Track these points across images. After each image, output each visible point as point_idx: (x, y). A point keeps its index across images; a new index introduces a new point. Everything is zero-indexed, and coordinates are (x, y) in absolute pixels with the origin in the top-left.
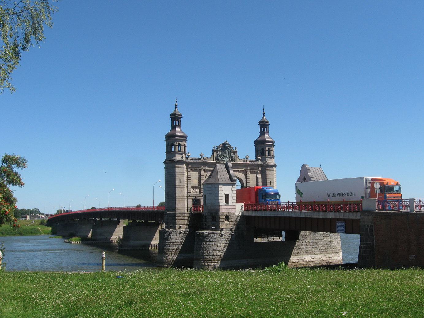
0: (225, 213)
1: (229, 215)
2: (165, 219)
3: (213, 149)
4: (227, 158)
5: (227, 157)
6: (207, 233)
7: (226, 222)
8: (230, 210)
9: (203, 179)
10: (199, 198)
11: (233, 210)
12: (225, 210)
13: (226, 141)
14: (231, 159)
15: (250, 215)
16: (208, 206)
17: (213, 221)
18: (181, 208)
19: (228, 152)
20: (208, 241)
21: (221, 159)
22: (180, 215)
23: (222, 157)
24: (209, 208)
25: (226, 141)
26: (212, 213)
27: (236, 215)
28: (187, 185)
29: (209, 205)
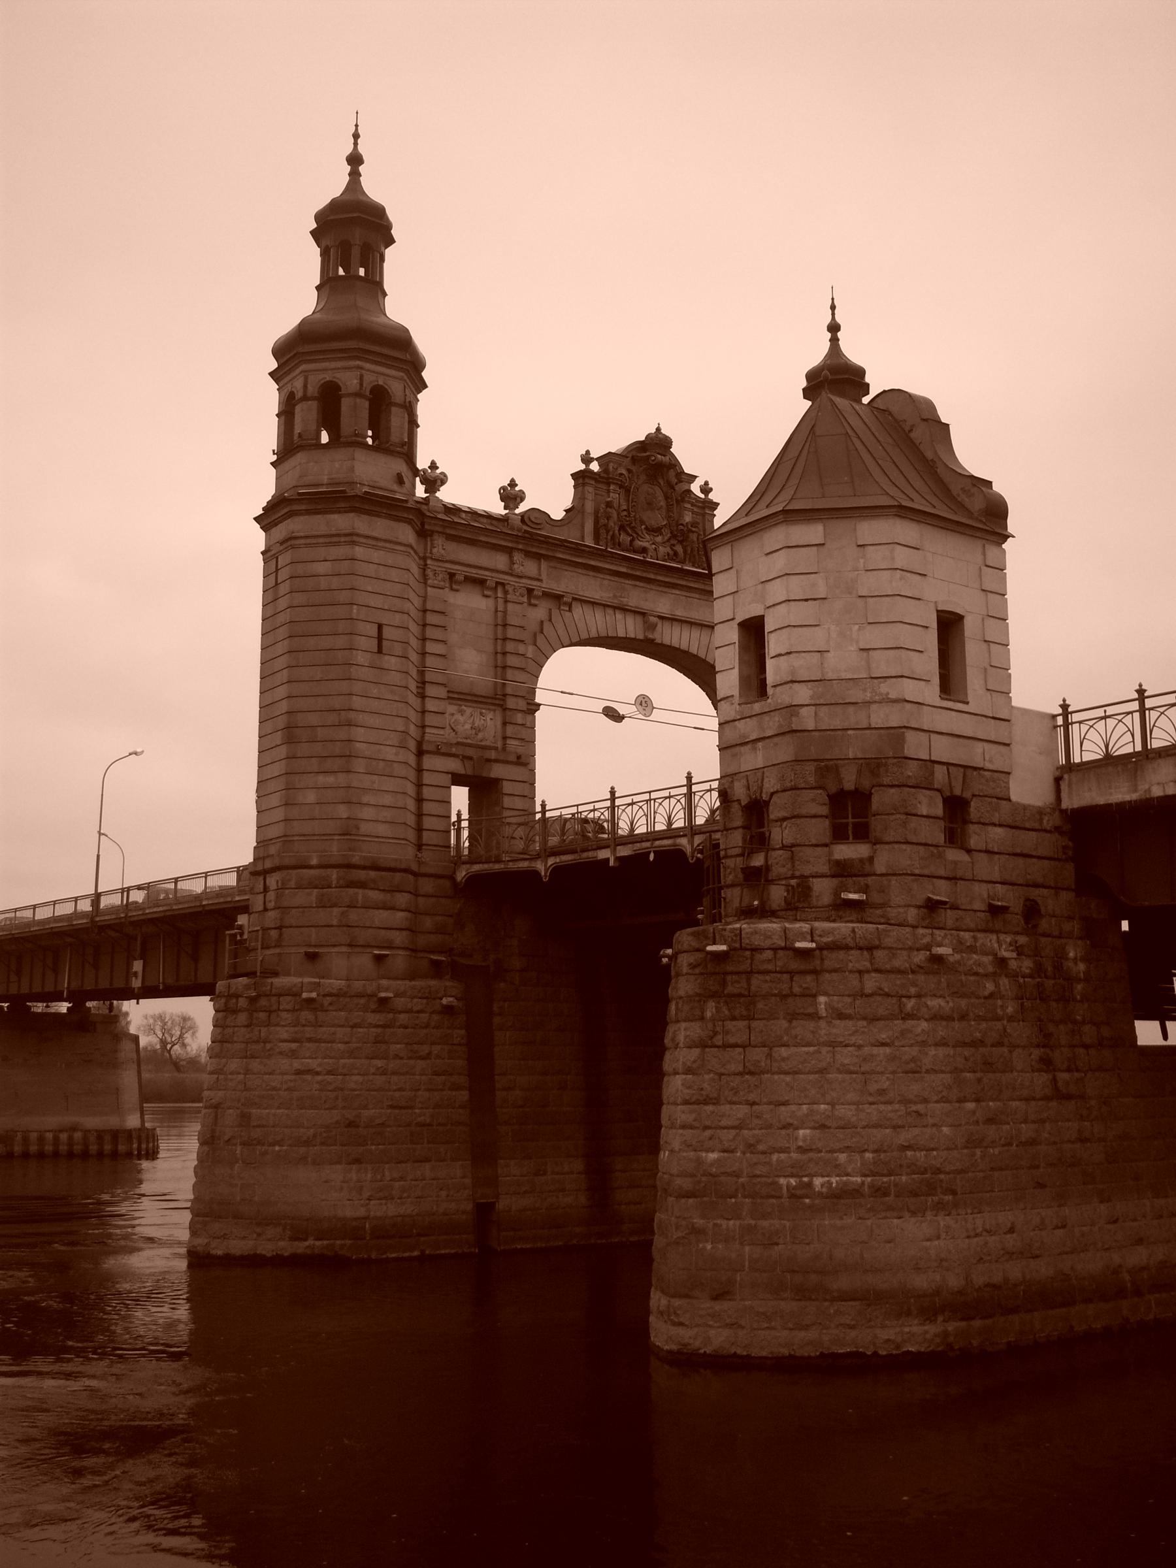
0: (940, 773)
1: (967, 795)
2: (261, 908)
3: (583, 467)
4: (659, 539)
5: (657, 531)
6: (802, 936)
7: (954, 855)
8: (977, 755)
9: (521, 648)
10: (493, 775)
11: (990, 757)
12: (942, 750)
13: (658, 429)
14: (679, 549)
15: (1157, 792)
16: (792, 709)
17: (839, 834)
18: (382, 829)
19: (663, 503)
20: (815, 1016)
21: (625, 538)
22: (372, 874)
23: (633, 528)
24: (807, 719)
25: (658, 429)
26: (827, 769)
27: (1014, 798)
28: (422, 673)
29: (802, 694)
